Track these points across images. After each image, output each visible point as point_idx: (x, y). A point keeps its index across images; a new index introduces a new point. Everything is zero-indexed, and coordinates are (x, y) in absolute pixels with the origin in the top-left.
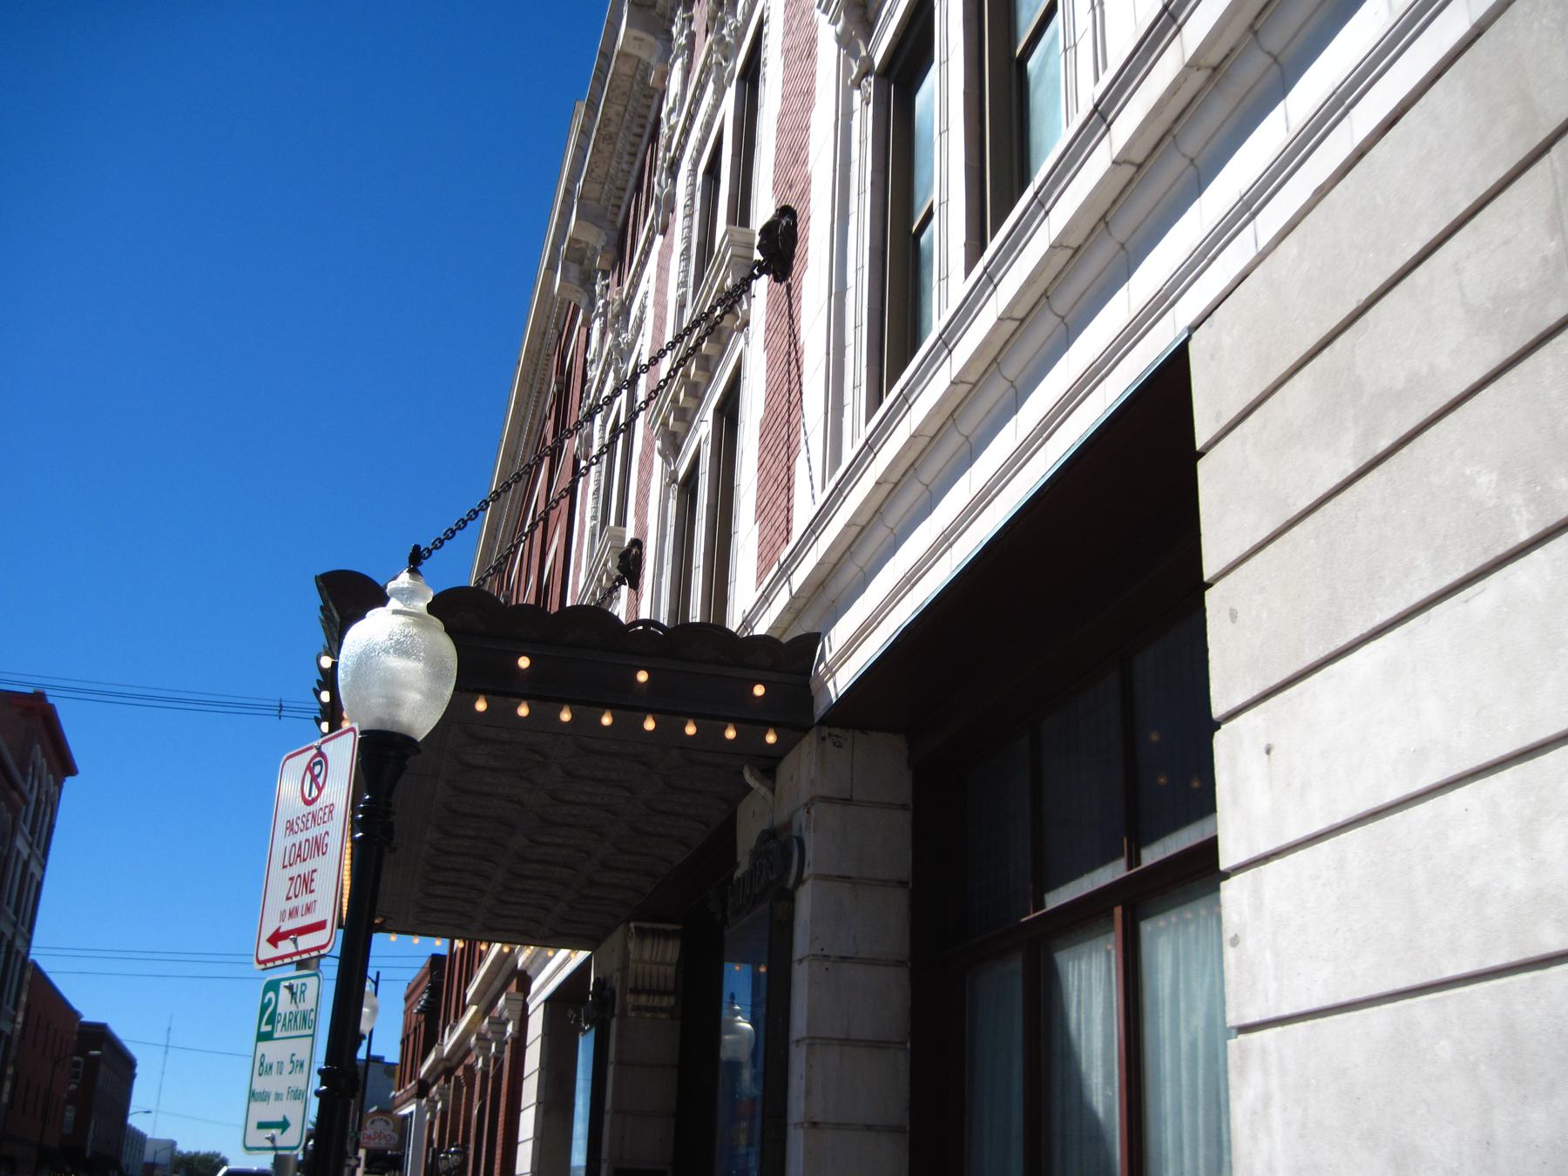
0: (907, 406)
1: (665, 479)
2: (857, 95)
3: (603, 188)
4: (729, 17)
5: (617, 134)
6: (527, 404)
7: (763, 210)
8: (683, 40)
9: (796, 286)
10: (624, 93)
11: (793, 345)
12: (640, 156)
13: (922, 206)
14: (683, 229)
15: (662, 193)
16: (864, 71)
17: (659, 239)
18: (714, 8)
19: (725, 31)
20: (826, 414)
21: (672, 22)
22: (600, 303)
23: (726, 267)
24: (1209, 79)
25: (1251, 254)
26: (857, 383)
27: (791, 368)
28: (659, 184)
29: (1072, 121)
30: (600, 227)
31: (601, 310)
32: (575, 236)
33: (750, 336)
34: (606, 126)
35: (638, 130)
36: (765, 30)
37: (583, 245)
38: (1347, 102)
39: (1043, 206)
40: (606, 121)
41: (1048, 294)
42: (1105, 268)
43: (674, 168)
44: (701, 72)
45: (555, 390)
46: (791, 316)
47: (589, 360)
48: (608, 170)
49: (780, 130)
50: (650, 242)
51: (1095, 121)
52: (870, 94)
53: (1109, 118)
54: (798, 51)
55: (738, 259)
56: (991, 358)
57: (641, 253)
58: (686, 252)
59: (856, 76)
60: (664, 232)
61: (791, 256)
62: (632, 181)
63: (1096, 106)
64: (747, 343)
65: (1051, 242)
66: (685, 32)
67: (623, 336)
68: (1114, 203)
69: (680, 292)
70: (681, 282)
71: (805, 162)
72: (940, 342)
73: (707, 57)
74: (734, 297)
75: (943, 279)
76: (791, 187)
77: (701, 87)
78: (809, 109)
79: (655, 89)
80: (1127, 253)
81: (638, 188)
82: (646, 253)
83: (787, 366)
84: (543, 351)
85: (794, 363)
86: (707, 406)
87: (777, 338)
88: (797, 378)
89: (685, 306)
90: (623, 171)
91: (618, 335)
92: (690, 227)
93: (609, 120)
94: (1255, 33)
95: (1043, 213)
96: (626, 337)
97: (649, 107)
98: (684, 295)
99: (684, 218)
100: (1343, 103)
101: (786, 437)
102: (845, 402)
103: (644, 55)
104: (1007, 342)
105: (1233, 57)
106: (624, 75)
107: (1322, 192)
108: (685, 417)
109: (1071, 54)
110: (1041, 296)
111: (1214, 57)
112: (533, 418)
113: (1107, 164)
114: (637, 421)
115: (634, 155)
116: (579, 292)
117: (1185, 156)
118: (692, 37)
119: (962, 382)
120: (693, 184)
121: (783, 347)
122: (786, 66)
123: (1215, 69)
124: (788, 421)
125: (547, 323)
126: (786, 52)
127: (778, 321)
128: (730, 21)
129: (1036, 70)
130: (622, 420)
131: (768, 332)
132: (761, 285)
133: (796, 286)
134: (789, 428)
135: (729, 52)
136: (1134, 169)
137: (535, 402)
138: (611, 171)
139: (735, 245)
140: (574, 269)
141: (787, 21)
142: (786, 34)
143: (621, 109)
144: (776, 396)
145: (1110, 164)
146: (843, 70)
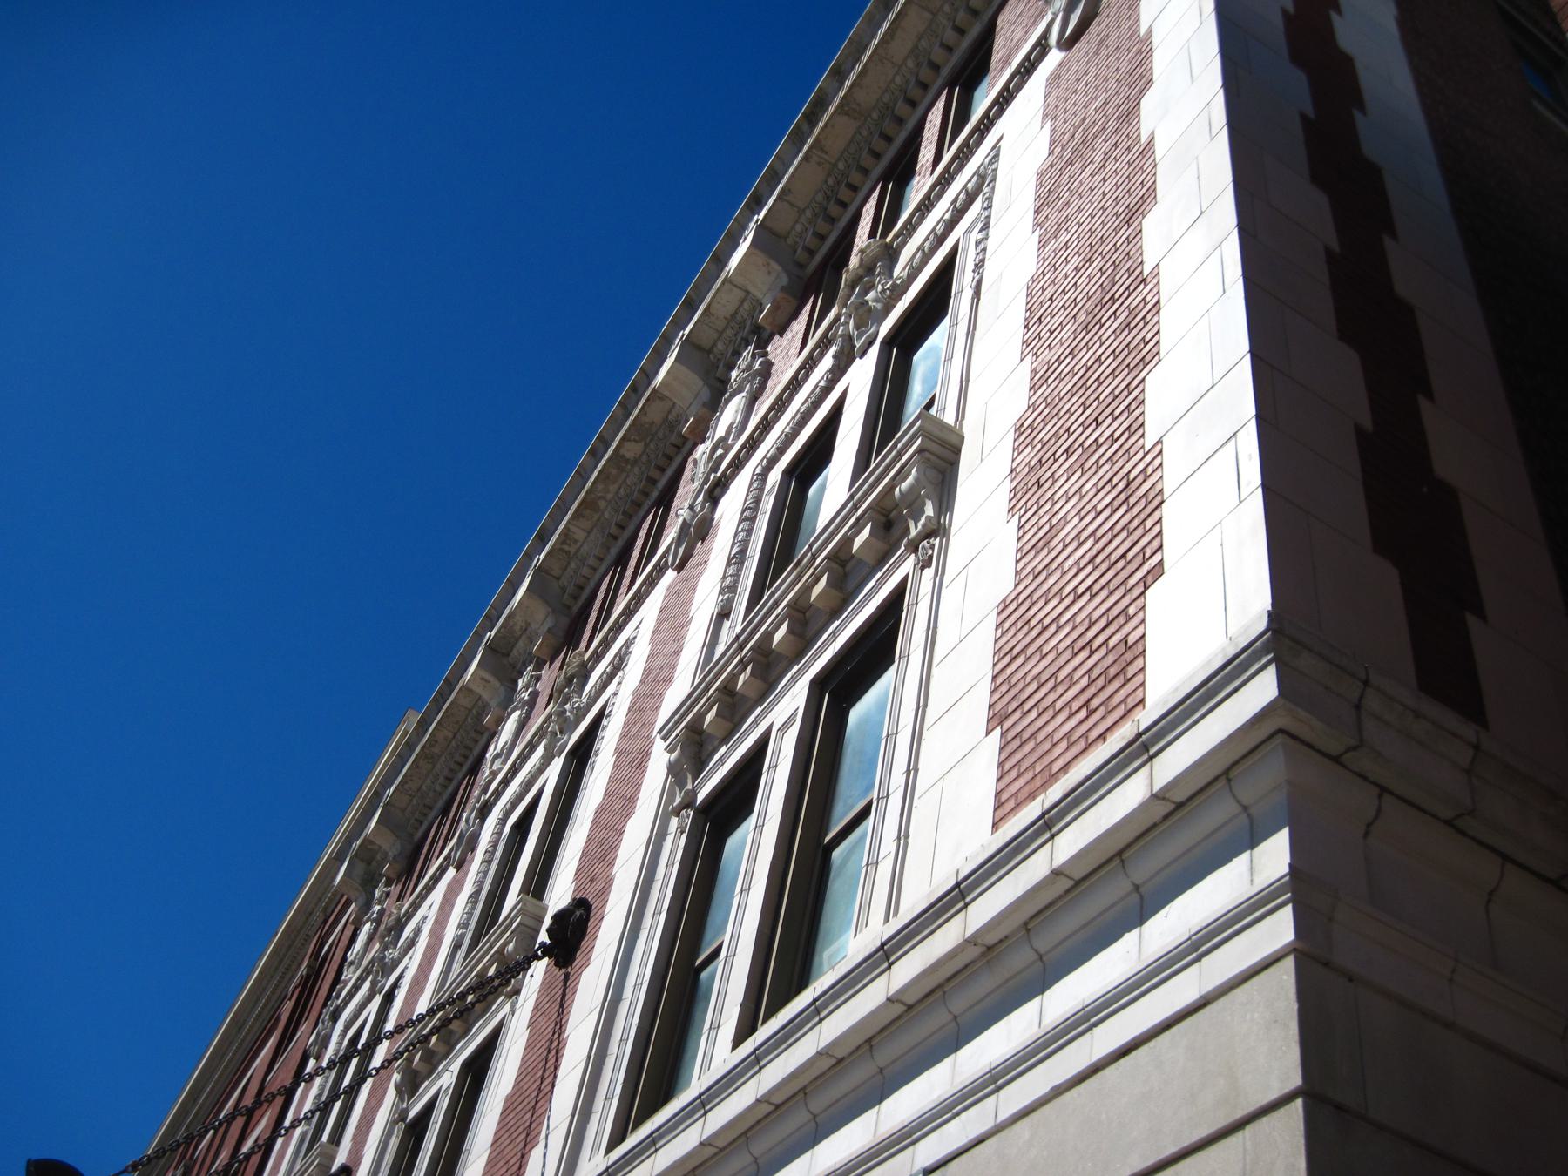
0: (653, 1149)
1: (394, 1115)
2: (674, 822)
3: (411, 800)
4: (575, 695)
5: (440, 756)
6: (272, 977)
7: (559, 894)
8: (526, 695)
9: (573, 978)
10: (457, 722)
11: (556, 1036)
12: (455, 782)
13: (710, 944)
14: (479, 873)
15: (468, 830)
16: (686, 802)
17: (451, 872)
18: (564, 683)
19: (567, 707)
20: (573, 1115)
21: (520, 675)
22: (377, 908)
23: (512, 932)
24: (983, 955)
25: (988, 1124)
26: (610, 1095)
27: (550, 1056)
28: (467, 821)
29: (860, 931)
30: (397, 836)
31: (375, 915)
32: (371, 838)
33: (517, 1006)
34: (431, 746)
35: (458, 758)
36: (605, 722)
37: (376, 847)
38: (1092, 1020)
39: (819, 1014)
40: (433, 741)
41: (807, 1091)
42: (863, 1083)
43: (486, 810)
44: (536, 734)
45: (304, 973)
46: (562, 1005)
47: (349, 960)
48: (421, 786)
49: (595, 823)
50: (442, 870)
51: (880, 957)
52: (687, 825)
53: (892, 959)
54: (630, 758)
55: (526, 929)
56: (742, 1131)
57: (431, 879)
58: (474, 897)
59: (678, 804)
60: (459, 867)
61: (577, 947)
62: (440, 804)
63: (883, 945)
64: (513, 1012)
65: (819, 1049)
66: (530, 690)
67: (390, 951)
68: (882, 1030)
69: (460, 932)
70: (463, 924)
71: (611, 864)
72: (698, 1101)
73: (545, 722)
74: (513, 970)
75: (714, 1028)
76: (592, 881)
77: (531, 747)
78: (628, 816)
79: (487, 729)
80: (884, 1078)
81: (445, 812)
82: (436, 879)
83: (546, 1052)
84: (304, 930)
85: (553, 1052)
86: (457, 1056)
87: (542, 1021)
88: (552, 1069)
89: (460, 947)
90: (435, 791)
91: (386, 948)
92: (485, 873)
93: (436, 742)
94: (1028, 930)
95: (817, 1019)
96: (392, 953)
97: (476, 741)
98: (462, 937)
99: (483, 862)
100: (1089, 1020)
101: (528, 1124)
102: (594, 1109)
103: (485, 695)
104: (759, 1121)
105: (1004, 945)
106: (462, 706)
107: (1058, 1091)
108: (433, 1061)
109: (871, 870)
110: (799, 1091)
111: (991, 939)
112: (273, 993)
113: (881, 999)
114: (379, 1047)
115: (450, 780)
116: (357, 889)
117: (950, 1012)
118: (535, 695)
119: (710, 1145)
120: (499, 833)
121: (547, 1031)
122: (616, 766)
123: (989, 948)
124: (534, 1107)
125: (316, 905)
126: (619, 752)
127: (548, 1005)
128: (575, 700)
129: (839, 862)
130: (363, 1040)
131: (536, 1011)
132: (540, 968)
133: (573, 978)
134: (532, 1116)
135: (567, 726)
136: (904, 1008)
137: (281, 977)
138: (424, 787)
139: (525, 914)
140: (360, 868)
141: (626, 724)
142: (623, 736)
143: (451, 735)
144: (528, 1078)
145: (885, 999)
146: (667, 796)
